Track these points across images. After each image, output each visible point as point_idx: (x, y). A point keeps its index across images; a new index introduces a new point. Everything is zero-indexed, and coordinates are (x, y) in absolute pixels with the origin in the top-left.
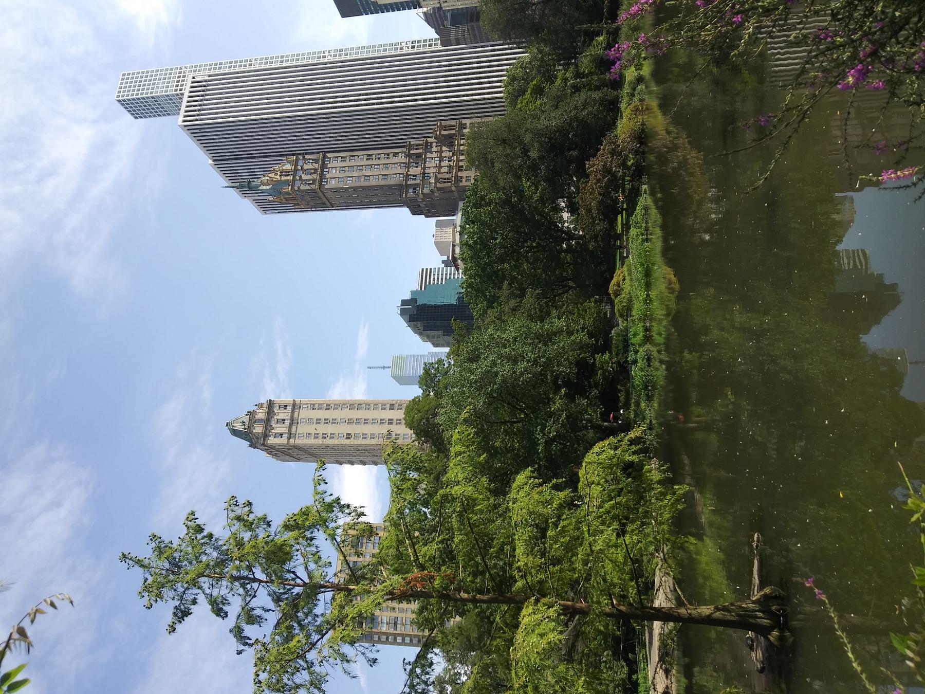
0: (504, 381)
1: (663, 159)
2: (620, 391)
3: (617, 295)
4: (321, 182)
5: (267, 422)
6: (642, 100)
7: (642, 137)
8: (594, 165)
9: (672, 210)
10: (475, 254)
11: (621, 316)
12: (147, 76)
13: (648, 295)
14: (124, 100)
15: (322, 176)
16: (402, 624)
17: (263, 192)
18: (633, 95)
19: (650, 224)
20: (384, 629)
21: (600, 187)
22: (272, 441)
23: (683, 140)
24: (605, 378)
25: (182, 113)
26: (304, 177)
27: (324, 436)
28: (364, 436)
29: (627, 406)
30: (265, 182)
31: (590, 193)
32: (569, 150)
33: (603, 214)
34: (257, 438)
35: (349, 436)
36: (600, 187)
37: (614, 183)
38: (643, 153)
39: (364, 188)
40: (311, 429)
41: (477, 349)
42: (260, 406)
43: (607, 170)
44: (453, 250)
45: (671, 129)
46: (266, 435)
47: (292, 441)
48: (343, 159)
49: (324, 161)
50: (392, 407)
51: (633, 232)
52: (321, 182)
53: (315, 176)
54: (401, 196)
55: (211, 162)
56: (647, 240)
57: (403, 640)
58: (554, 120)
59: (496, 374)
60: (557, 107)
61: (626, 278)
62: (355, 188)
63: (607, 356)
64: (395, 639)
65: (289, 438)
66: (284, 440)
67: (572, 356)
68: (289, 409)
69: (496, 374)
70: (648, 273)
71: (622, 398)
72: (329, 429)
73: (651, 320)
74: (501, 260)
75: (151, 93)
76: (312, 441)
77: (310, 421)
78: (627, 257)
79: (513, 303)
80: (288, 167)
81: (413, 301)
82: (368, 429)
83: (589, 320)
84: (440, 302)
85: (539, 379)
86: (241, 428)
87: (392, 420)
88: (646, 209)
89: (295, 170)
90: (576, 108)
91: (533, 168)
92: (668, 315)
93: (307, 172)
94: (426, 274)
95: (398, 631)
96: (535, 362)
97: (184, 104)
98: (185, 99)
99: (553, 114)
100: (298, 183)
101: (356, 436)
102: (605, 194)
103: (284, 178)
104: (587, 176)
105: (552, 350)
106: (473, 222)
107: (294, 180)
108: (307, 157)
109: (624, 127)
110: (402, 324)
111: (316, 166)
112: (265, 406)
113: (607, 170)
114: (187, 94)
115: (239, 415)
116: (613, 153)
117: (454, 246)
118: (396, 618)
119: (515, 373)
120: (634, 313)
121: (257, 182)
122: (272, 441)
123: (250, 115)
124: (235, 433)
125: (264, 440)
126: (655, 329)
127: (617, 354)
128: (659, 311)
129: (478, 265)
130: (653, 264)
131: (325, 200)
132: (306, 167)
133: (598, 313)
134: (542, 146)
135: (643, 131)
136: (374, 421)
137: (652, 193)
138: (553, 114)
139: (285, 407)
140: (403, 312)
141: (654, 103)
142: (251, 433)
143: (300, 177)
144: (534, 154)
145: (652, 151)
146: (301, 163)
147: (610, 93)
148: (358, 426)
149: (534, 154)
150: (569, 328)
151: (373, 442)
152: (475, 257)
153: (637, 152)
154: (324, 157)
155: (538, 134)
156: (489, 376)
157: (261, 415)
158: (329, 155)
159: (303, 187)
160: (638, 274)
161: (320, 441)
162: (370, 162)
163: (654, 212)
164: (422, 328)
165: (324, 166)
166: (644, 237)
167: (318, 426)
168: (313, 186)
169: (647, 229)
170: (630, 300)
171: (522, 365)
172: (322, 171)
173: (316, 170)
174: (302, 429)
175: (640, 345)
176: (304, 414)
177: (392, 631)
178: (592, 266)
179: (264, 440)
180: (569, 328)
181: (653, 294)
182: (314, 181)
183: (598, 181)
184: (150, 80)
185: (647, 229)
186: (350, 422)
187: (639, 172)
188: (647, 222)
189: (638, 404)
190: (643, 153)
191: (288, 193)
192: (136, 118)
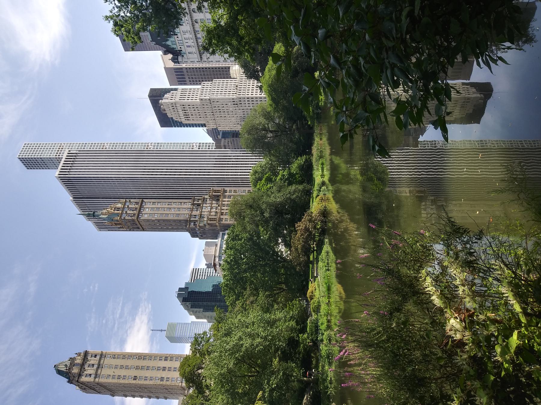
0: (247, 350)
1: (335, 226)
2: (313, 357)
3: (312, 299)
4: (138, 215)
5: (82, 366)
6: (325, 195)
7: (325, 213)
8: (300, 226)
9: (340, 252)
10: (231, 267)
11: (314, 311)
13: (329, 301)
18: (320, 191)
19: (329, 261)
21: (303, 238)
22: (84, 379)
23: (346, 217)
24: (305, 349)
25: (59, 170)
26: (128, 212)
27: (119, 377)
29: (317, 367)
30: (103, 214)
31: (298, 240)
32: (286, 214)
33: (304, 252)
35: (135, 378)
36: (303, 238)
37: (310, 236)
38: (326, 222)
39: (164, 220)
40: (110, 372)
41: (231, 328)
42: (79, 354)
43: (307, 230)
44: (214, 260)
45: (340, 211)
46: (80, 375)
47: (97, 380)
49: (142, 204)
50: (166, 359)
51: (320, 264)
52: (138, 215)
53: (135, 212)
54: (186, 226)
55: (71, 198)
56: (328, 270)
58: (277, 198)
59: (242, 345)
60: (279, 191)
61: (317, 289)
62: (159, 220)
63: (306, 336)
65: (95, 378)
66: (91, 379)
67: (286, 334)
68: (98, 357)
69: (242, 345)
70: (329, 289)
71: (314, 362)
72: (123, 372)
73: (331, 315)
74: (245, 271)
76: (110, 380)
77: (110, 367)
78: (317, 277)
79: (252, 299)
80: (119, 205)
81: (186, 288)
82: (148, 374)
83: (295, 312)
85: (267, 349)
87: (174, 371)
88: (328, 253)
89: (124, 208)
90: (290, 193)
91: (266, 222)
92: (340, 312)
93: (131, 209)
94: (195, 272)
96: (265, 338)
97: (61, 164)
98: (62, 162)
99: (278, 195)
100: (124, 215)
102: (306, 241)
103: (116, 212)
104: (296, 231)
105: (275, 331)
106: (231, 249)
107: (122, 214)
108: (132, 200)
109: (315, 207)
111: (137, 206)
112: (82, 354)
113: (307, 230)
114: (63, 159)
116: (310, 221)
117: (215, 257)
119: (253, 345)
120: (321, 311)
121: (99, 212)
122: (84, 379)
123: (101, 174)
124: (59, 372)
125: (78, 378)
126: (333, 321)
127: (312, 335)
128: (335, 311)
129: (232, 273)
130: (332, 284)
131: (139, 226)
132: (130, 206)
133: (300, 307)
134: (271, 211)
135: (325, 210)
136: (153, 368)
137: (330, 244)
138: (278, 195)
139: (95, 356)
140: (179, 296)
141: (330, 195)
143: (126, 212)
144: (267, 215)
145: (330, 221)
146: (127, 204)
147: (308, 187)
149: (267, 215)
150: (283, 318)
151: (151, 383)
152: (231, 269)
153: (322, 222)
155: (269, 205)
156: (237, 347)
157: (79, 361)
158: (145, 200)
160: (323, 289)
161: (115, 381)
162: (169, 206)
163: (331, 254)
164: (190, 306)
166: (327, 268)
167: (116, 370)
168: (133, 218)
169: (328, 264)
170: (319, 302)
171: (259, 340)
173: (136, 208)
174: (105, 372)
175: (325, 331)
176: (107, 361)
178: (297, 280)
179: (78, 378)
180: (283, 318)
181: (332, 300)
182: (134, 214)
183: (302, 235)
185: (328, 264)
186: (137, 368)
187: (324, 232)
188: (328, 260)
189: (323, 367)
190: (326, 222)
191: (117, 221)
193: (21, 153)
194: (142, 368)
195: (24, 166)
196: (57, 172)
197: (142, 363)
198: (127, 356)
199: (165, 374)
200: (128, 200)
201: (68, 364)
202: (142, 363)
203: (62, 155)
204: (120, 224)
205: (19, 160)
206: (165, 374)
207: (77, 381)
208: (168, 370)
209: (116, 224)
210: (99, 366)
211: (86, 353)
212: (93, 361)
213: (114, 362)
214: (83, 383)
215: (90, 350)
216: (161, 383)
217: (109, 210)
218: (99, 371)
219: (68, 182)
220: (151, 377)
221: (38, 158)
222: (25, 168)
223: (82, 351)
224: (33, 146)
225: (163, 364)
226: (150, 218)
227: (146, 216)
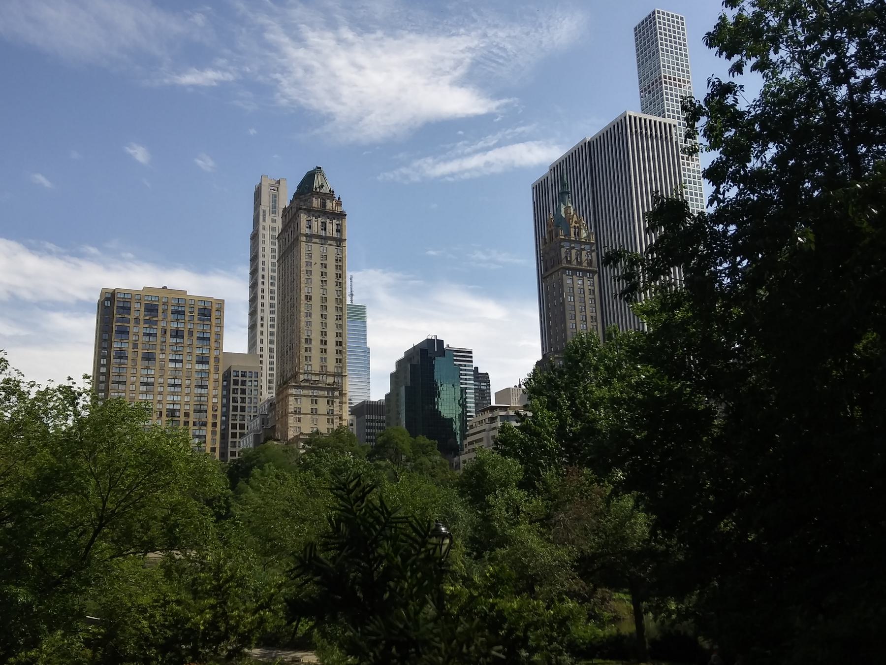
4: (569, 269)
5: (322, 212)
12: (680, 44)
14: (654, 19)
15: (575, 270)
16: (120, 364)
17: (558, 209)
20: (116, 346)
22: (304, 218)
25: (640, 114)
26: (574, 252)
28: (309, 315)
34: (306, 200)
35: (309, 298)
39: (563, 313)
40: (316, 259)
42: (339, 204)
44: (501, 408)
46: (310, 211)
47: (304, 239)
48: (592, 292)
49: (590, 271)
50: (339, 343)
52: (569, 269)
53: (575, 263)
54: (556, 352)
55: (588, 139)
57: (103, 366)
62: (563, 304)
64: (104, 357)
65: (306, 235)
66: (304, 230)
68: (336, 235)
72: (316, 278)
75: (662, 50)
76: (304, 259)
77: (324, 257)
80: (584, 234)
82: (316, 318)
84: (435, 374)
86: (316, 184)
93: (579, 255)
94: (466, 355)
95: (113, 360)
97: (648, 117)
98: (653, 118)
100: (566, 245)
101: (309, 306)
103: (572, 230)
108: (594, 254)
110: (417, 339)
111: (585, 264)
112: (339, 209)
114: (658, 119)
115: (332, 181)
117: (505, 408)
118: (126, 358)
121: (568, 200)
122: (304, 218)
124: (310, 177)
125: (305, 209)
132: (584, 253)
140: (429, 342)
142: (312, 195)
143: (573, 248)
146: (587, 247)
148: (319, 308)
151: (303, 324)
154: (593, 272)
158: (596, 277)
159: (563, 250)
161: (303, 268)
162: (589, 319)
164: (415, 362)
165: (584, 272)
167: (319, 265)
172: (580, 270)
173: (580, 263)
174: (316, 249)
176: (331, 251)
177: (113, 354)
179: (305, 209)
182: (570, 262)
184: (676, 48)
186: (324, 299)
191: (557, 235)
192: (635, 29)
193: (663, 14)
194: (324, 308)
195: (639, 21)
196: (635, 111)
197: (331, 305)
198: (340, 280)
199: (316, 345)
200: (594, 248)
201: (325, 190)
202: (331, 305)
203: (669, 116)
204: (551, 239)
205: (650, 12)
206: (316, 345)
207: (300, 209)
208: (322, 349)
209: (550, 232)
210: (324, 239)
211: (342, 215)
212: (331, 227)
213: (331, 262)
214: (296, 216)
215: (348, 223)
216: (303, 341)
217: (575, 219)
218: (316, 240)
219: (618, 132)
220: (311, 324)
221: (657, 46)
222: (636, 24)
223: (344, 208)
224: (679, 33)
225: (331, 339)
226: (566, 290)
227: (569, 282)
